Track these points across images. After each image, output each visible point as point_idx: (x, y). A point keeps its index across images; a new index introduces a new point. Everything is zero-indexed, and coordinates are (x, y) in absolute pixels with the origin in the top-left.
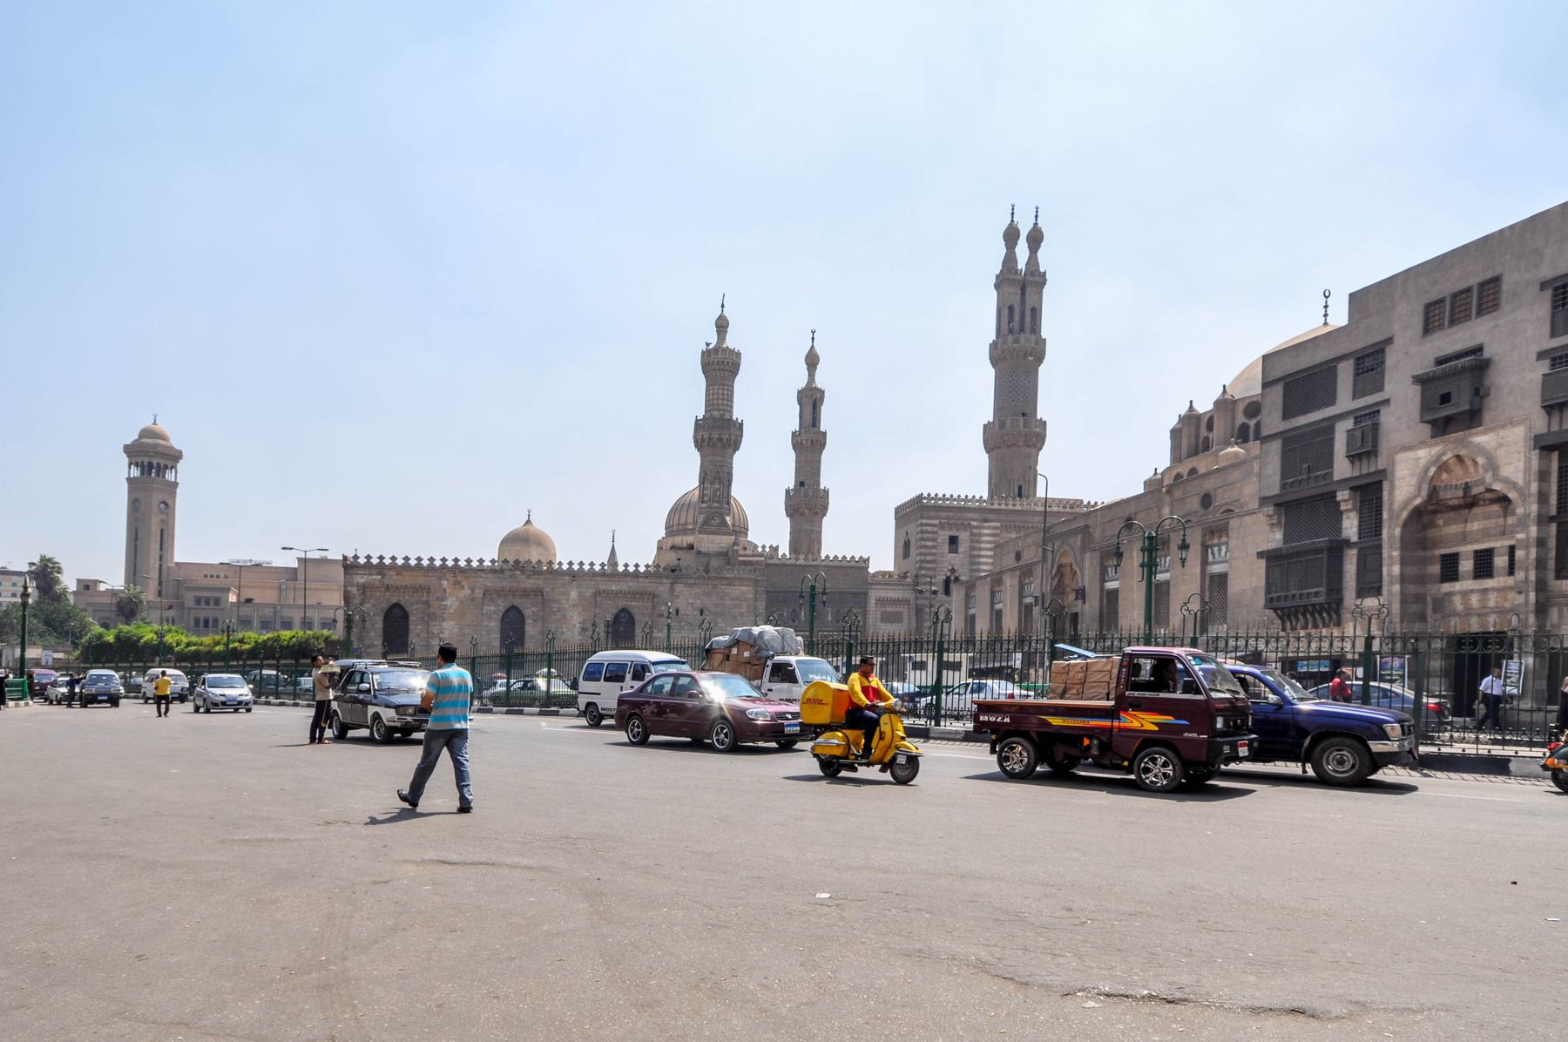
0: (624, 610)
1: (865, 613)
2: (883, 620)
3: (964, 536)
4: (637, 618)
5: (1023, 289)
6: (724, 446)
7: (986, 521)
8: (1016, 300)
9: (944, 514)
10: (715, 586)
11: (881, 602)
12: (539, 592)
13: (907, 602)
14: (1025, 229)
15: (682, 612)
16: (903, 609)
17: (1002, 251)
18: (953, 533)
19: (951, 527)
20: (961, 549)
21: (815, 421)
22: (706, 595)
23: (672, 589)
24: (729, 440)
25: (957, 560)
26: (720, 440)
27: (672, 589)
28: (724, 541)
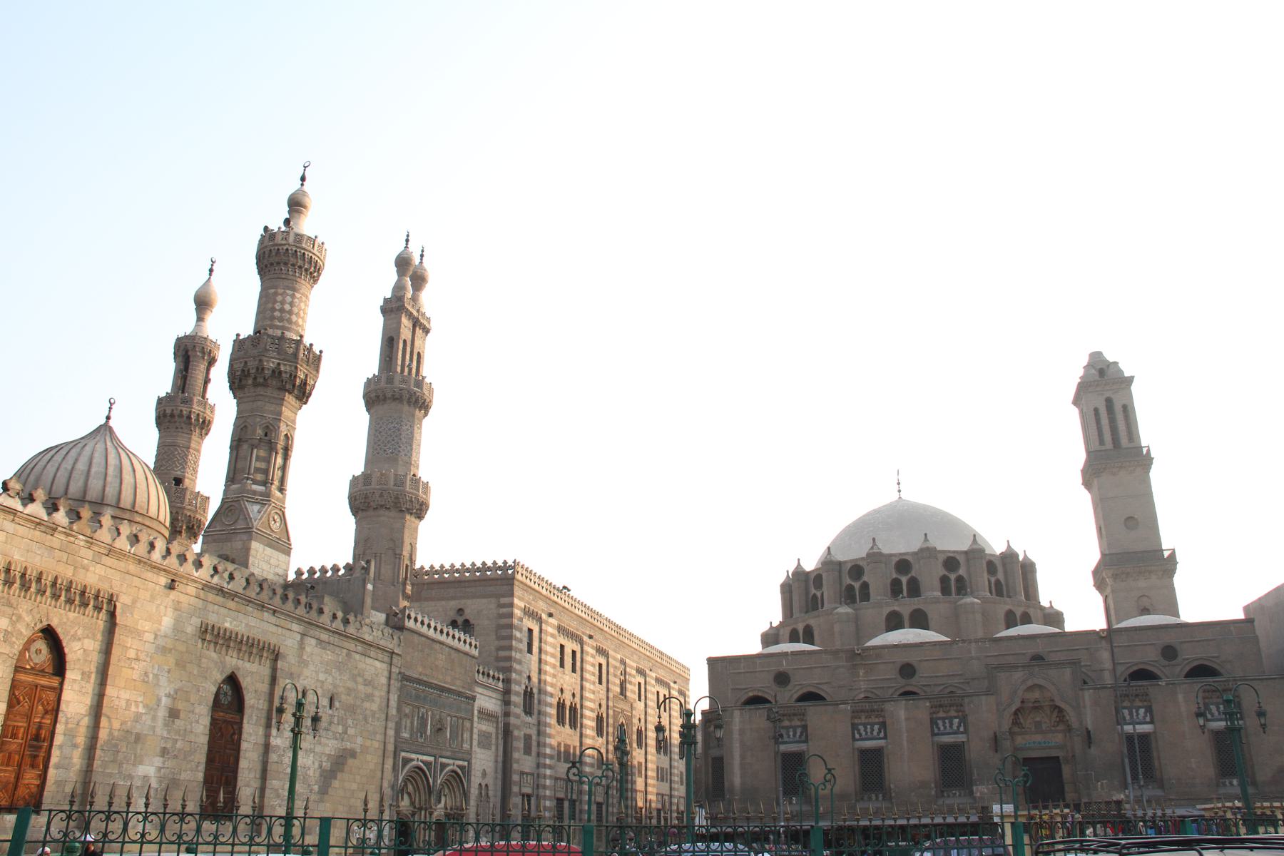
5: (414, 326)
22: (340, 666)
23: (302, 646)
27: (302, 646)
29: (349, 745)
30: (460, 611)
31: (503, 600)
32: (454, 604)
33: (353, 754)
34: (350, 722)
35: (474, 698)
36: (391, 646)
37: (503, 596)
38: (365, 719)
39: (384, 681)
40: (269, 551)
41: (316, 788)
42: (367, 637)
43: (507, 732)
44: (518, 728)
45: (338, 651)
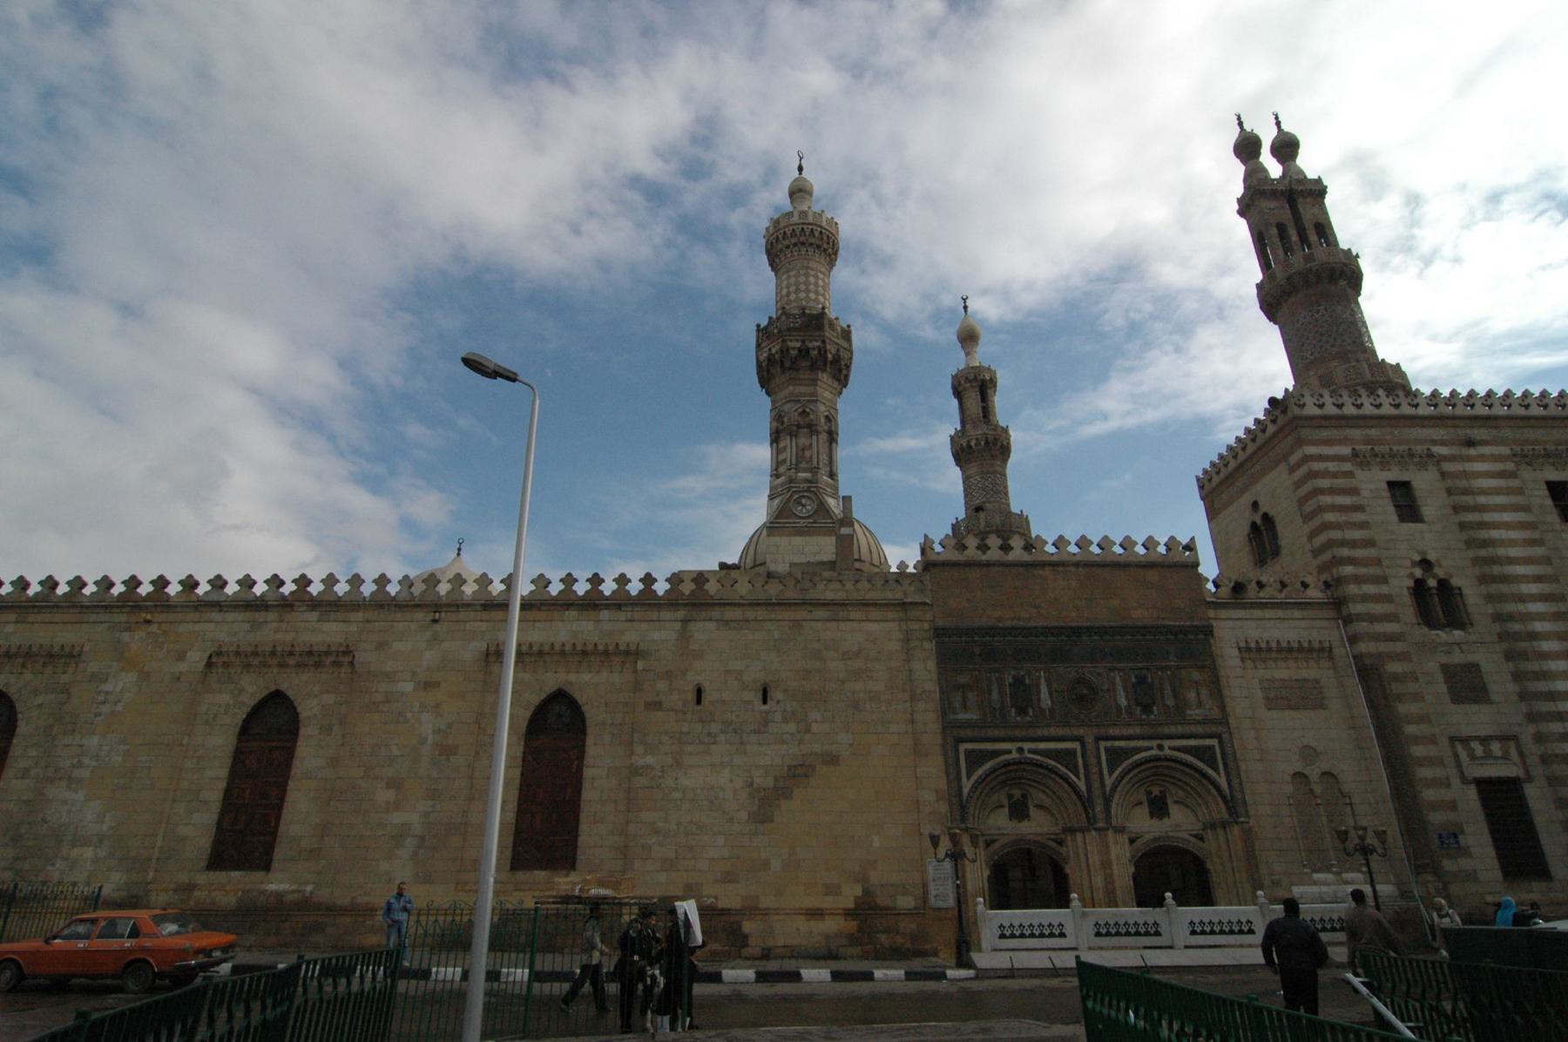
0: (560, 697)
1: (1216, 687)
2: (1272, 703)
3: (1424, 482)
4: (594, 715)
6: (814, 367)
7: (1470, 443)
8: (1286, 215)
9: (1356, 433)
10: (797, 624)
11: (1252, 652)
12: (343, 657)
13: (1323, 652)
14: (1267, 137)
15: (706, 699)
16: (1309, 671)
17: (1239, 169)
18: (1395, 474)
19: (1385, 461)
20: (1428, 511)
21: (987, 412)
24: (822, 353)
25: (1433, 537)
26: (804, 352)
27: (684, 636)
28: (823, 548)
29: (817, 748)
30: (1255, 505)
31: (1293, 459)
32: (1247, 499)
33: (833, 760)
34: (814, 715)
35: (1208, 631)
36: (899, 595)
37: (1291, 453)
38: (856, 705)
39: (894, 646)
40: (798, 541)
41: (744, 815)
42: (830, 595)
43: (1368, 673)
44: (1402, 657)
45: (769, 625)
